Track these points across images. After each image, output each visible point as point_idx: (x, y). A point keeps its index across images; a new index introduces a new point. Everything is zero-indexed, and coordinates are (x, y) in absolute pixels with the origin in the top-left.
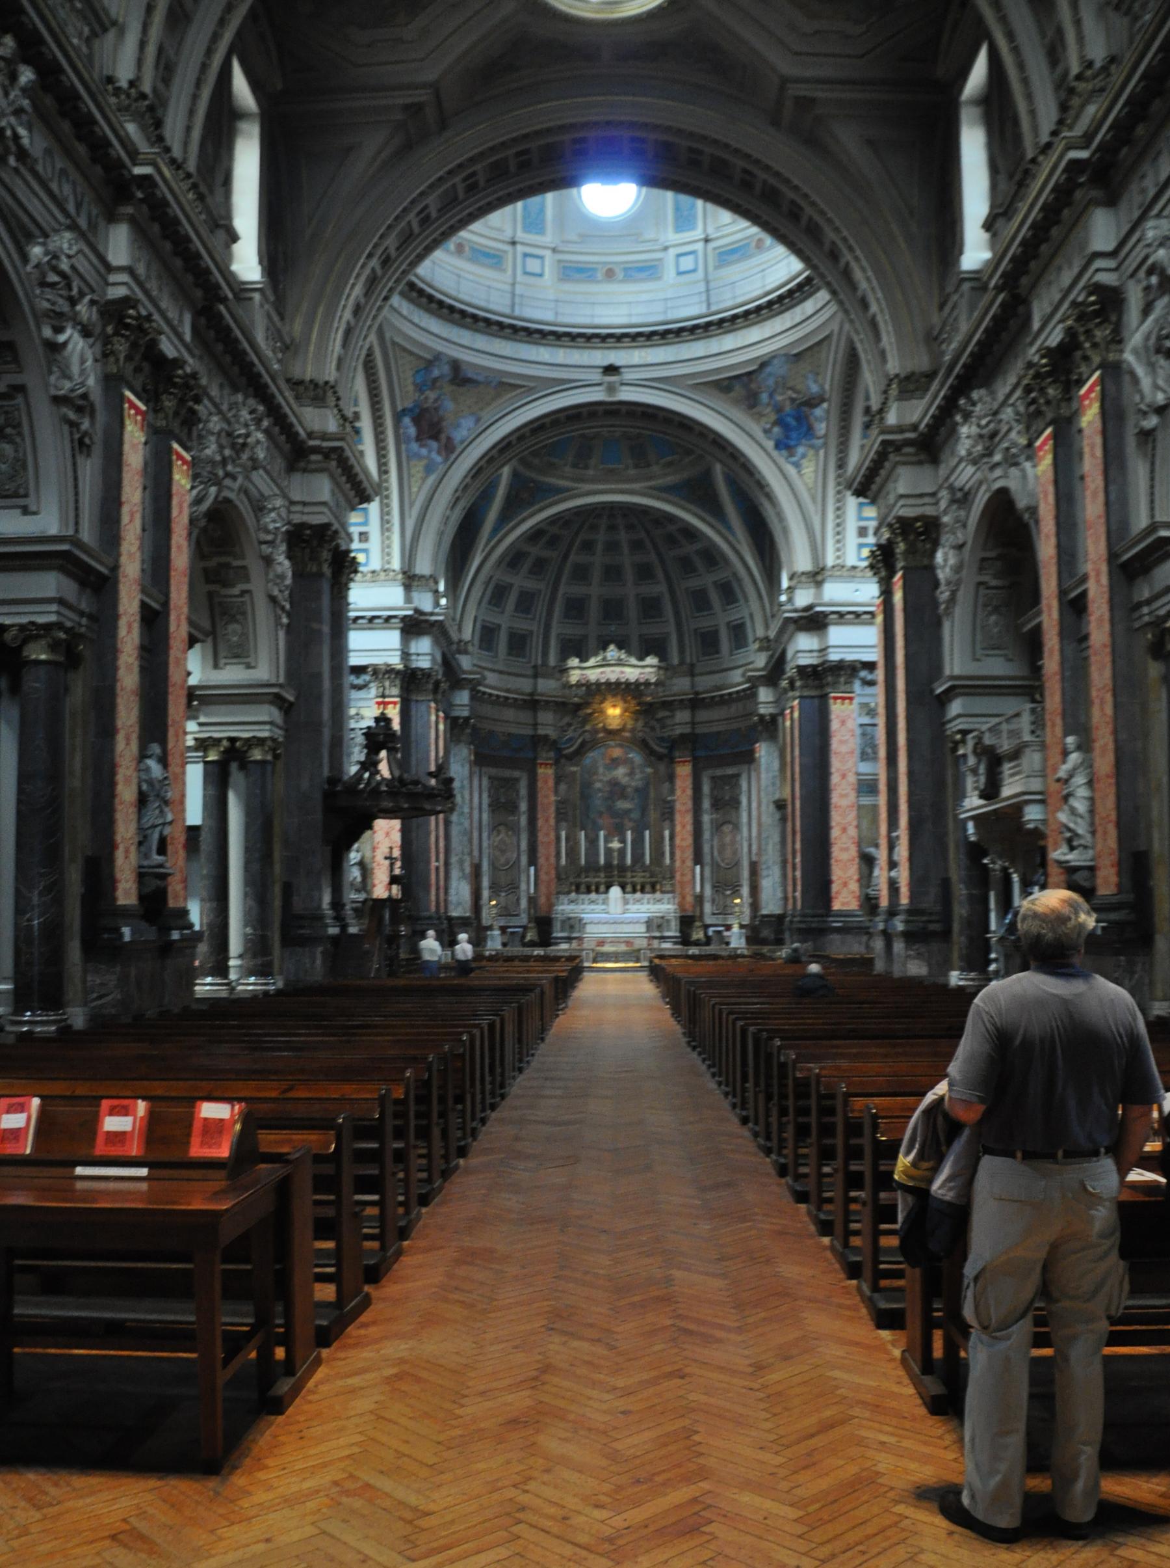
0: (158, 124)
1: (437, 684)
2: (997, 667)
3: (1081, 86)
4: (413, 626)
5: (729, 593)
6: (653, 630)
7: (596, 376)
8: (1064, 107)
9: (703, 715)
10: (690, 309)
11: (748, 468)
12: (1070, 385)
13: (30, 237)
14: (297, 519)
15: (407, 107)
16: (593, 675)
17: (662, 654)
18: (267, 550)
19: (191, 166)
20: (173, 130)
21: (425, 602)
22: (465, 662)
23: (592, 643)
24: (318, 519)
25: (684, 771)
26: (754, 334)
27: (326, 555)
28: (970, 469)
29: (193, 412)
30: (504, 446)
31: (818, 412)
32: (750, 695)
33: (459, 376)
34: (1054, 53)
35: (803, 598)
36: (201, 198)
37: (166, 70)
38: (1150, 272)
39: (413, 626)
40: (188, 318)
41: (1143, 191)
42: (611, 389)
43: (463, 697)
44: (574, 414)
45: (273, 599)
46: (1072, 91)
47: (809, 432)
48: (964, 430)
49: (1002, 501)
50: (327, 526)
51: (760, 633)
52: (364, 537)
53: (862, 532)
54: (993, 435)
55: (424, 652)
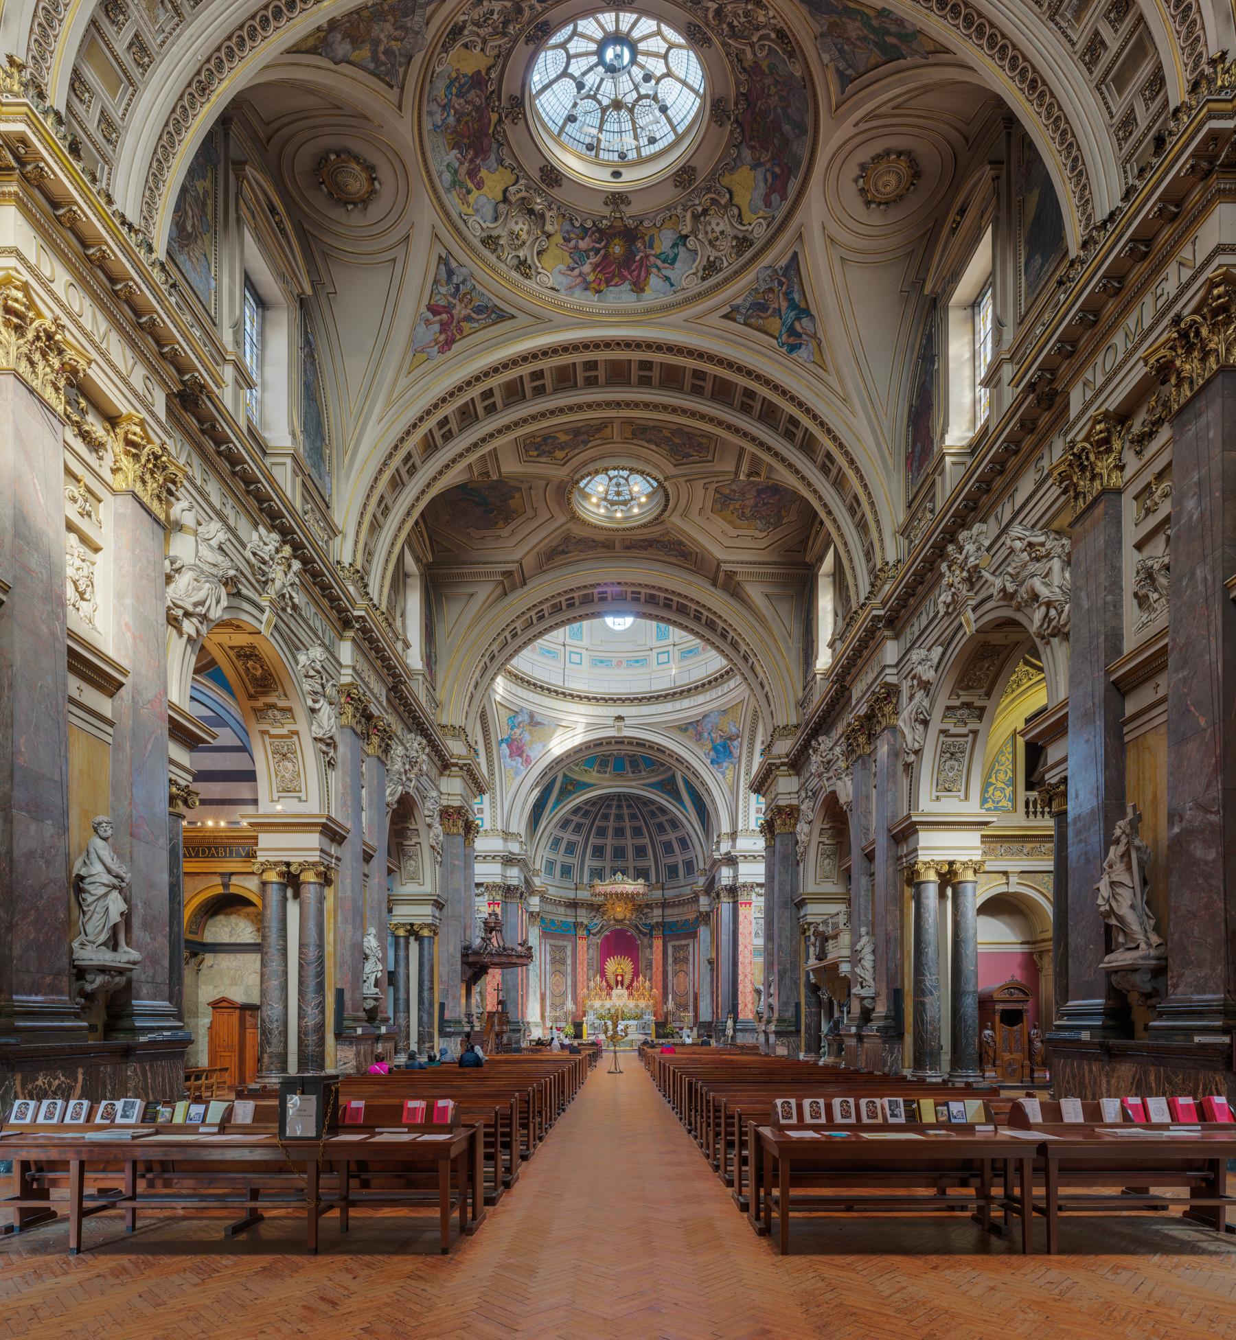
0: (366, 586)
1: (522, 894)
2: (831, 888)
3: (881, 575)
5: (684, 843)
6: (641, 864)
8: (873, 585)
9: (668, 911)
12: (871, 738)
13: (298, 649)
14: (445, 803)
16: (609, 889)
17: (647, 878)
18: (428, 820)
19: (383, 608)
20: (373, 590)
21: (515, 848)
22: (537, 881)
23: (608, 871)
24: (457, 804)
25: (658, 943)
27: (460, 823)
28: (817, 780)
29: (388, 745)
32: (695, 899)
34: (869, 555)
35: (725, 847)
36: (390, 625)
37: (369, 554)
38: (913, 678)
39: (509, 860)
40: (384, 692)
41: (913, 633)
43: (535, 901)
45: (432, 847)
46: (876, 577)
48: (814, 758)
49: (833, 798)
50: (462, 807)
51: (701, 866)
52: (481, 811)
54: (828, 762)
55: (514, 876)
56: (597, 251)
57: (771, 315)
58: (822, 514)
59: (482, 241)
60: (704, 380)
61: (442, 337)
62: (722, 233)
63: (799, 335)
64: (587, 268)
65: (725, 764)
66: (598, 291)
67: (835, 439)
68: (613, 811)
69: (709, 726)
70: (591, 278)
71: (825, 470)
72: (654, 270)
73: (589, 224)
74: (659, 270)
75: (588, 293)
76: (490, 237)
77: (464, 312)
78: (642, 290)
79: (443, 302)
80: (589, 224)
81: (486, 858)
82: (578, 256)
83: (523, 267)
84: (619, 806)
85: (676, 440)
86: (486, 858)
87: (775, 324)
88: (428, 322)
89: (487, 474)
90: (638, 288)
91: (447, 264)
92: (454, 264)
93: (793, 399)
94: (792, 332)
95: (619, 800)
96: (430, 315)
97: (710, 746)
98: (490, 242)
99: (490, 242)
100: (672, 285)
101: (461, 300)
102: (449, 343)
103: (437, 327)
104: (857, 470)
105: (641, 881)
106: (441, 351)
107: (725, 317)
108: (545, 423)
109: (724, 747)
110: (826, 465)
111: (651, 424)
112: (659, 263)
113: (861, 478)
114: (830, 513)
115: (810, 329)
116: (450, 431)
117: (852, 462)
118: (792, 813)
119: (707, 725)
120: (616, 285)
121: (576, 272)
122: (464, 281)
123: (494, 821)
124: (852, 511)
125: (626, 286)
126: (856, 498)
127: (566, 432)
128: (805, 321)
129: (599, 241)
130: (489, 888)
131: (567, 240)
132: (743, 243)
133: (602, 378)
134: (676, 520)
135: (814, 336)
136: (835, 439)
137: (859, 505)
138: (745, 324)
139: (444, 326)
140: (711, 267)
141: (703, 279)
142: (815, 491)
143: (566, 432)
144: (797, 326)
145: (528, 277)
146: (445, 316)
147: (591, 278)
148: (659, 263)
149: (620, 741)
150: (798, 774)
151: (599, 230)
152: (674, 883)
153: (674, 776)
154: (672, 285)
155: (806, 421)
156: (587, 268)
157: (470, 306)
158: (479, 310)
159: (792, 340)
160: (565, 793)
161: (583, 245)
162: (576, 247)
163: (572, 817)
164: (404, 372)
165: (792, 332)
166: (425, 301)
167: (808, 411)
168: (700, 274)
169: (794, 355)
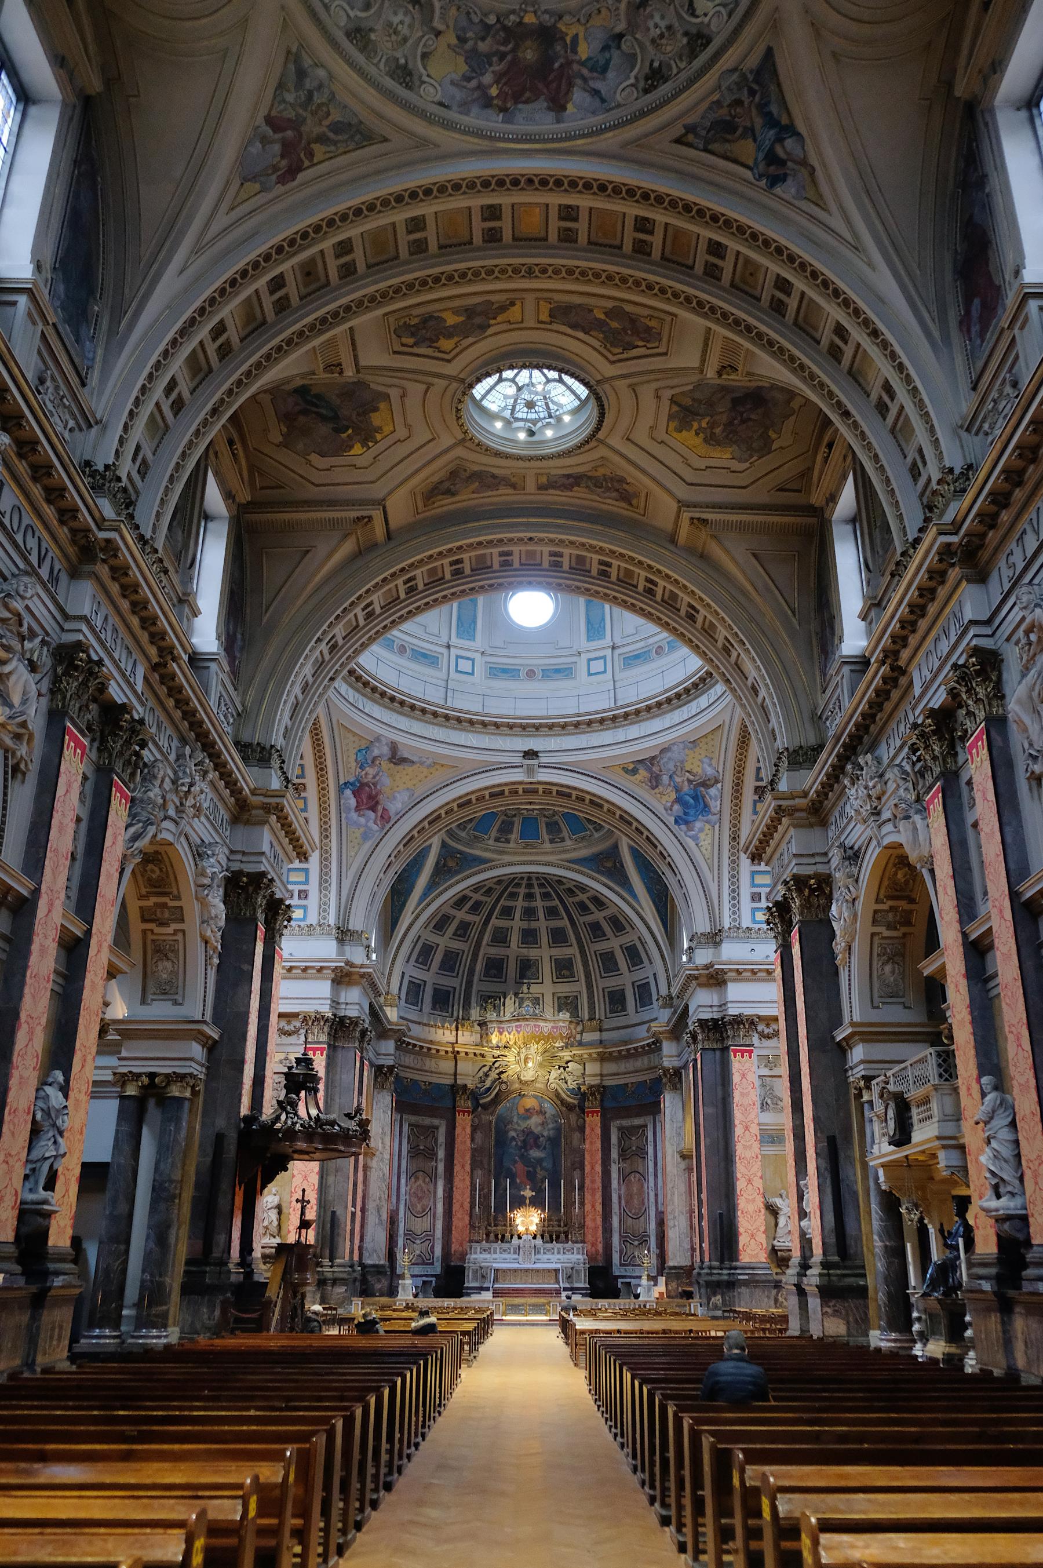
1: (364, 1033)
4: (342, 977)
7: (518, 759)
10: (599, 703)
11: (652, 842)
21: (356, 955)
22: (392, 1014)
26: (656, 724)
30: (434, 819)
31: (713, 791)
32: (655, 1047)
33: (397, 758)
35: (703, 956)
39: (342, 977)
42: (530, 771)
44: (497, 793)
47: (706, 809)
53: (756, 897)
56: (502, 56)
57: (743, 136)
59: (348, 35)
61: (284, 163)
62: (669, 28)
63: (782, 163)
64: (487, 79)
65: (698, 825)
66: (503, 110)
68: (520, 904)
69: (671, 766)
70: (494, 92)
72: (579, 81)
73: (492, 20)
74: (585, 80)
75: (490, 111)
76: (358, 30)
77: (317, 130)
78: (564, 108)
79: (291, 114)
80: (492, 20)
81: (304, 971)
82: (477, 62)
83: (404, 74)
84: (529, 896)
85: (614, 325)
86: (304, 971)
87: (747, 149)
88: (264, 140)
90: (558, 106)
91: (298, 60)
92: (307, 62)
94: (772, 159)
95: (530, 886)
96: (269, 131)
97: (673, 796)
98: (358, 34)
99: (358, 34)
100: (603, 100)
101: (314, 113)
102: (292, 172)
103: (277, 148)
105: (565, 1015)
106: (282, 180)
107: (678, 141)
109: (695, 798)
111: (577, 300)
112: (585, 72)
115: (798, 152)
116: (286, 297)
119: (668, 765)
120: (526, 102)
121: (474, 83)
122: (320, 86)
123: (323, 907)
125: (542, 104)
127: (456, 312)
128: (789, 143)
129: (505, 43)
130: (310, 1021)
131: (463, 40)
132: (699, 40)
134: (615, 441)
135: (804, 163)
138: (706, 150)
139: (288, 148)
140: (655, 76)
141: (646, 91)
144: (779, 151)
145: (409, 87)
146: (289, 133)
147: (494, 92)
148: (585, 72)
149: (531, 790)
151: (505, 28)
152: (621, 1021)
153: (616, 846)
154: (603, 100)
156: (487, 79)
157: (326, 123)
158: (337, 128)
159: (772, 168)
161: (483, 47)
162: (474, 50)
163: (453, 912)
164: (224, 207)
165: (772, 159)
166: (263, 112)
168: (642, 84)
169: (778, 190)
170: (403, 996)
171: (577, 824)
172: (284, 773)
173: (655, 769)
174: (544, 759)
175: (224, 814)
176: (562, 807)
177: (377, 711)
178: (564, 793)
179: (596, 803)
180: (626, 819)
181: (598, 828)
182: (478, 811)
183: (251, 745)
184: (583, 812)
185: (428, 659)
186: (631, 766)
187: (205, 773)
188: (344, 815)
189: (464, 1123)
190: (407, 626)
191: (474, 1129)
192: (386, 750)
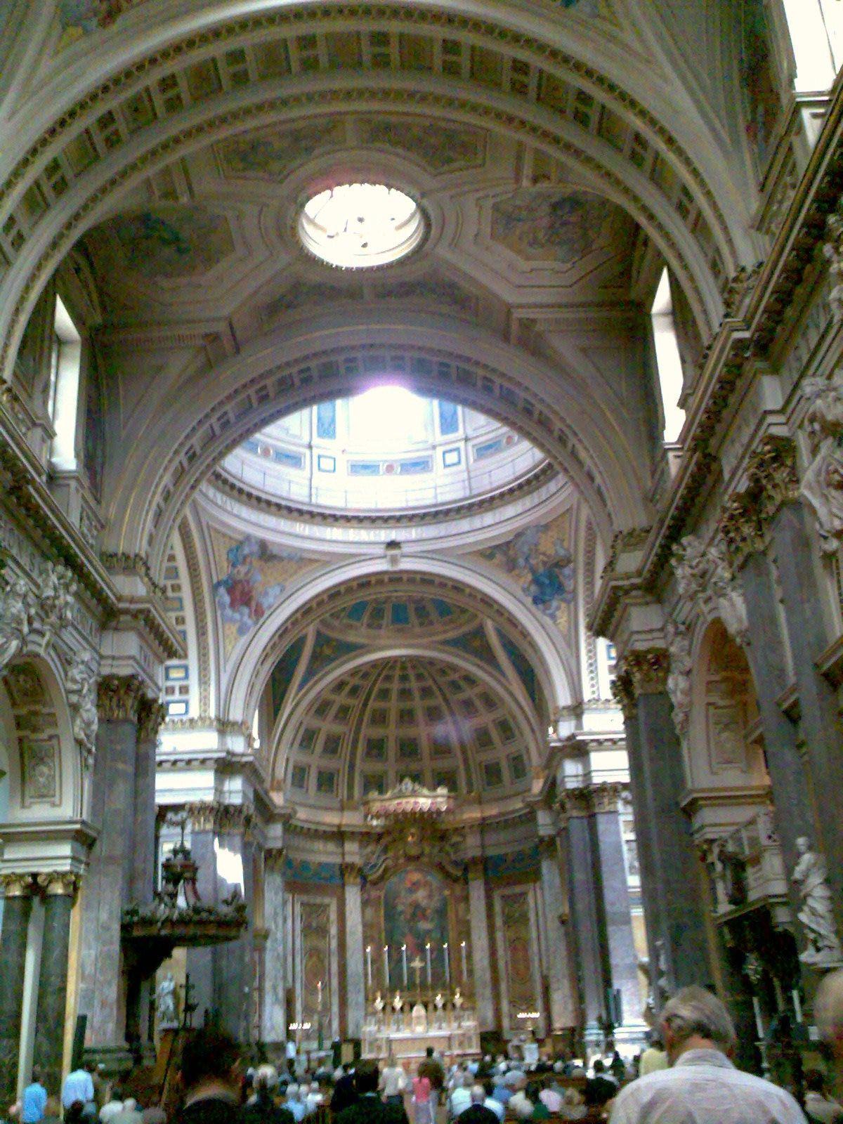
7: (379, 550)
15: (206, 336)
42: (394, 560)
58: (642, 220)
60: (457, 53)
67: (643, 113)
71: (635, 158)
89: (170, 194)
93: (578, 66)
104: (680, 152)
108: (250, 124)
110: (637, 151)
113: (688, 162)
114: (651, 217)
117: (670, 141)
118: (659, 661)
124: (682, 210)
126: (686, 191)
133: (324, 61)
136: (643, 113)
137: (691, 200)
142: (626, 191)
143: (282, 135)
150: (659, 600)
155: (599, 95)
160: (319, 660)
163: (333, 697)
167: (601, 80)
170: (289, 780)
171: (444, 609)
172: (150, 579)
173: (511, 552)
174: (406, 549)
175: (92, 622)
176: (430, 593)
177: (245, 512)
178: (427, 579)
179: (458, 587)
180: (487, 601)
181: (463, 611)
182: (348, 602)
183: (116, 555)
184: (450, 598)
185: (293, 460)
186: (488, 552)
187: (67, 586)
188: (219, 613)
189: (353, 897)
190: (270, 429)
191: (365, 903)
192: (256, 548)
